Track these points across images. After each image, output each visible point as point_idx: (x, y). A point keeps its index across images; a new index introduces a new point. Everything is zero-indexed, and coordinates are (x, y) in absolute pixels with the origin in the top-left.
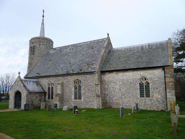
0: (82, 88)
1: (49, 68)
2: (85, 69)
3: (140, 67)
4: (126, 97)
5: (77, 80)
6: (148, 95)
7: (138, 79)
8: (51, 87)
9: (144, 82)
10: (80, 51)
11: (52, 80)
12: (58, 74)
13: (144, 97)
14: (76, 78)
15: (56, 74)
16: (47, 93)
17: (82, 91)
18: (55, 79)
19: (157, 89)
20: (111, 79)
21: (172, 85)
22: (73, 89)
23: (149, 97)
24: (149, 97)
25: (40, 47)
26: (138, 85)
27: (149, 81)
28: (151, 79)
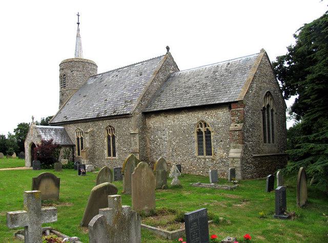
0: (116, 139)
2: (121, 111)
3: (197, 105)
5: (110, 126)
6: (209, 153)
7: (194, 124)
9: (203, 129)
11: (81, 127)
12: (87, 118)
13: (203, 154)
15: (86, 118)
16: (77, 146)
18: (84, 125)
19: (221, 141)
20: (157, 125)
21: (239, 135)
22: (106, 141)
25: (75, 74)
27: (210, 129)
28: (213, 124)
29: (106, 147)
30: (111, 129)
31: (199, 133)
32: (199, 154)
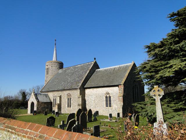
0: (72, 99)
1: (55, 85)
4: (98, 107)
6: (110, 106)
8: (55, 99)
9: (108, 96)
10: (76, 71)
11: (56, 94)
13: (108, 106)
14: (68, 93)
17: (72, 102)
22: (67, 100)
23: (111, 106)
24: (111, 106)
26: (105, 98)
29: (67, 103)
30: (69, 95)
31: (106, 97)
32: (106, 106)
